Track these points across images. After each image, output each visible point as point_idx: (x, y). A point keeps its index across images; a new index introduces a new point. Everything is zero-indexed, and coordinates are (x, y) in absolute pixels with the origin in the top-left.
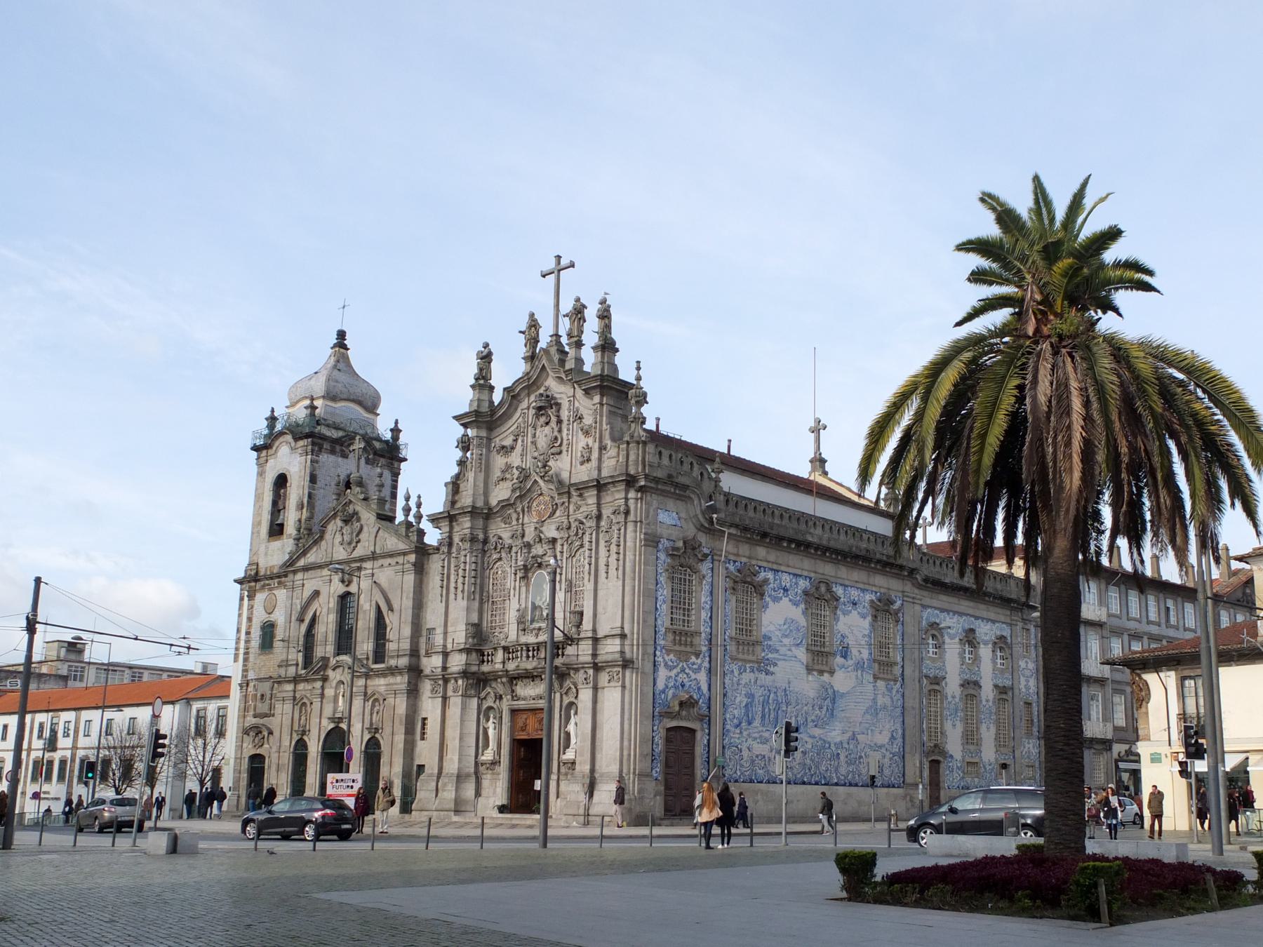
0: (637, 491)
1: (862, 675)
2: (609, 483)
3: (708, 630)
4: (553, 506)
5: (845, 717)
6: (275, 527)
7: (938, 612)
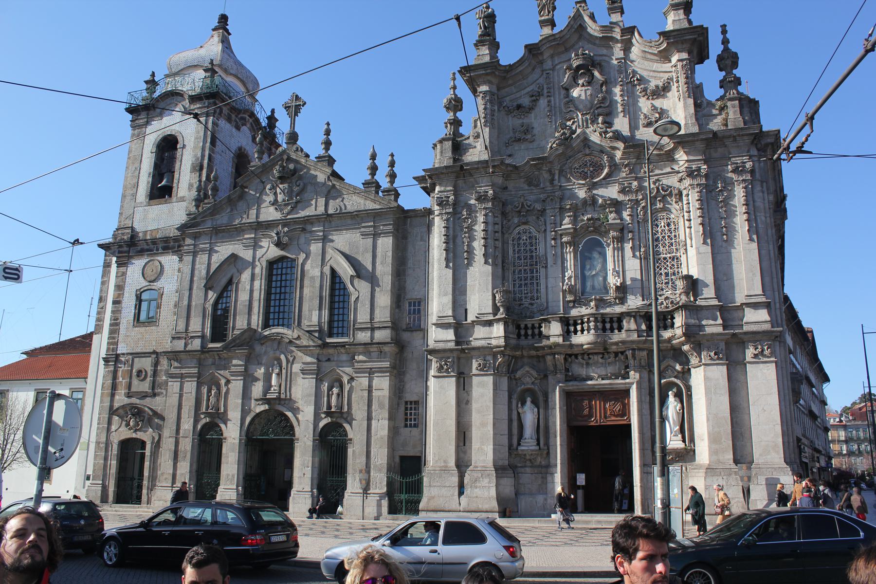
0: (758, 150)
2: (729, 137)
4: (610, 167)
6: (155, 191)
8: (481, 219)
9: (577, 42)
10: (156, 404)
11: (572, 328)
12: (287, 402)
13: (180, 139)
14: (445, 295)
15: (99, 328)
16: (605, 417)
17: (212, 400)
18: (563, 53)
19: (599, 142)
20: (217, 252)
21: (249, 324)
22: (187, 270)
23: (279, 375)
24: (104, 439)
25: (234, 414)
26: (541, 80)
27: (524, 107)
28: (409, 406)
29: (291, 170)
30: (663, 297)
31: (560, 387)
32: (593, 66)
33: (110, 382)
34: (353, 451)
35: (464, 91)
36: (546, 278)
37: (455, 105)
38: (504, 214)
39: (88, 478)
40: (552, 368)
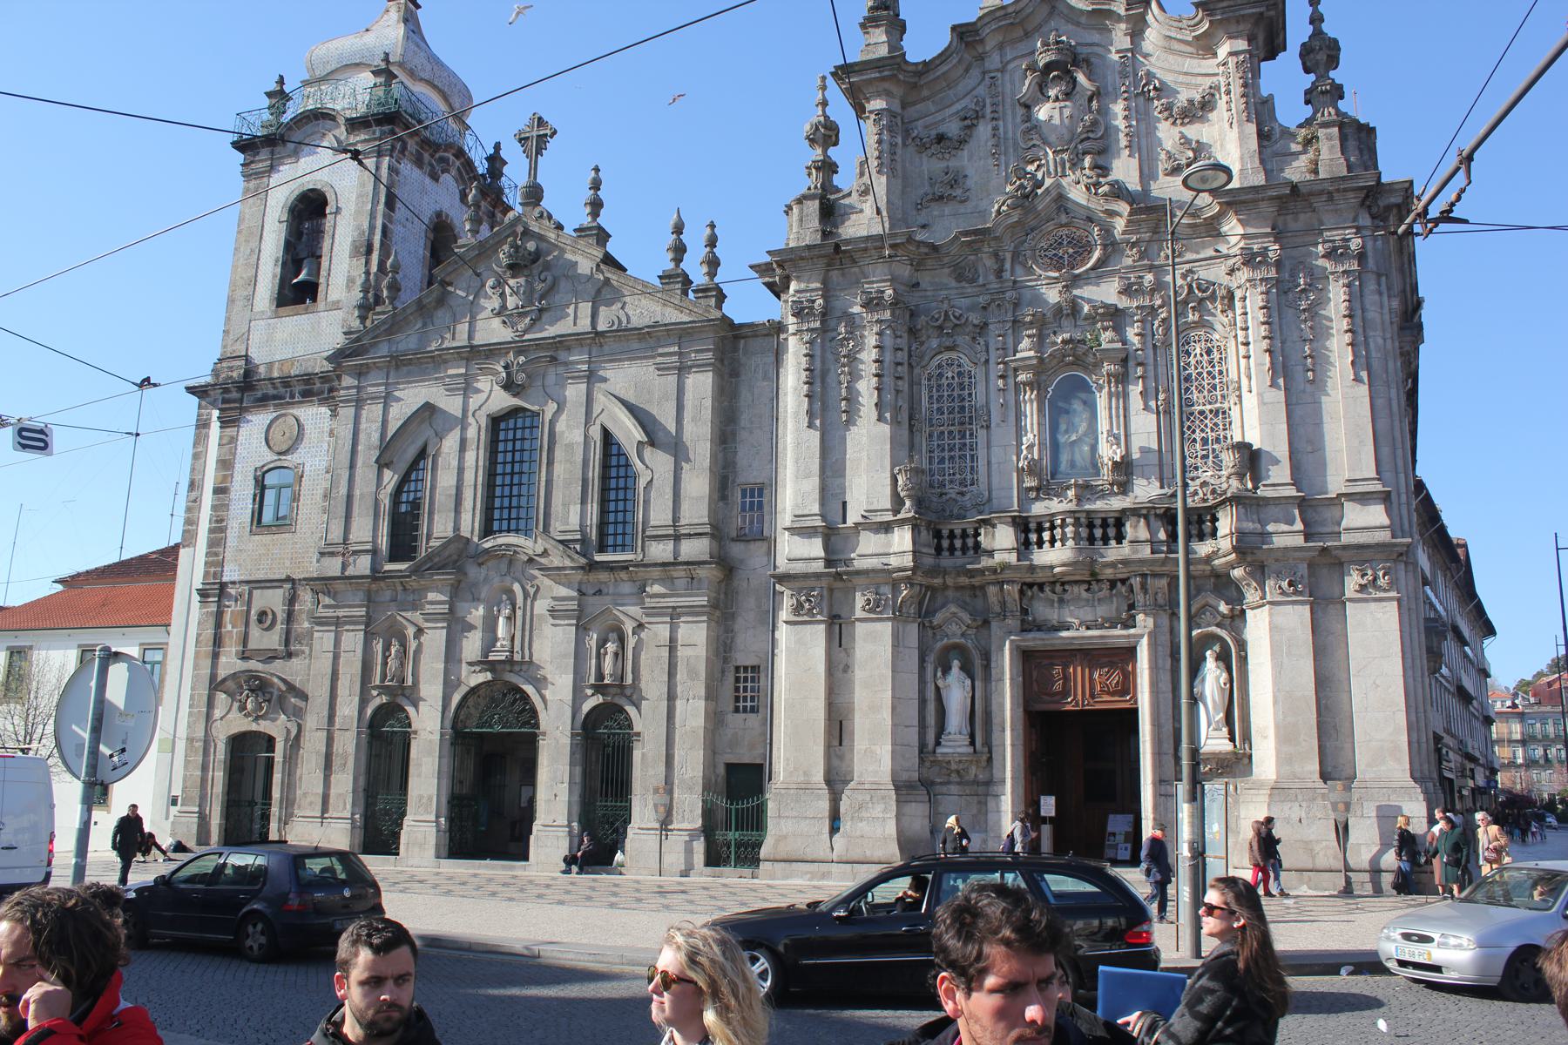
0: (1373, 217)
2: (1321, 193)
4: (1105, 246)
8: (871, 340)
9: (1046, 21)
10: (293, 670)
11: (1033, 537)
12: (524, 667)
13: (330, 197)
14: (807, 477)
15: (189, 537)
16: (1092, 696)
17: (392, 663)
18: (1020, 40)
19: (1084, 202)
20: (398, 400)
21: (457, 528)
22: (345, 432)
23: (511, 619)
24: (201, 734)
25: (431, 689)
26: (981, 90)
27: (950, 139)
28: (742, 675)
29: (530, 253)
30: (1198, 482)
31: (1012, 641)
32: (1076, 63)
33: (210, 632)
34: (643, 754)
35: (842, 110)
36: (989, 447)
37: (826, 134)
38: (913, 332)
39: (174, 802)
40: (997, 609)
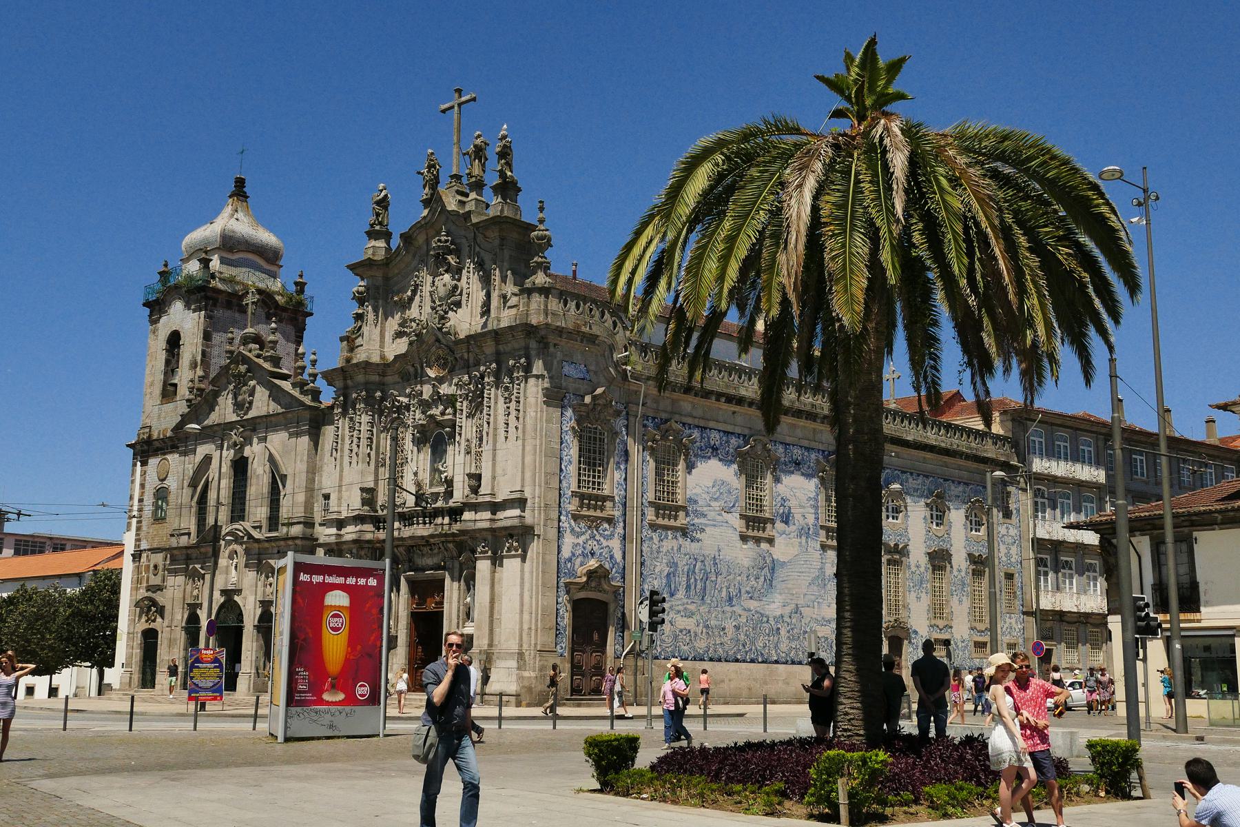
1: (807, 542)
3: (623, 492)
5: (787, 588)
6: (169, 388)
7: (899, 473)
13: (182, 335)
22: (181, 470)
